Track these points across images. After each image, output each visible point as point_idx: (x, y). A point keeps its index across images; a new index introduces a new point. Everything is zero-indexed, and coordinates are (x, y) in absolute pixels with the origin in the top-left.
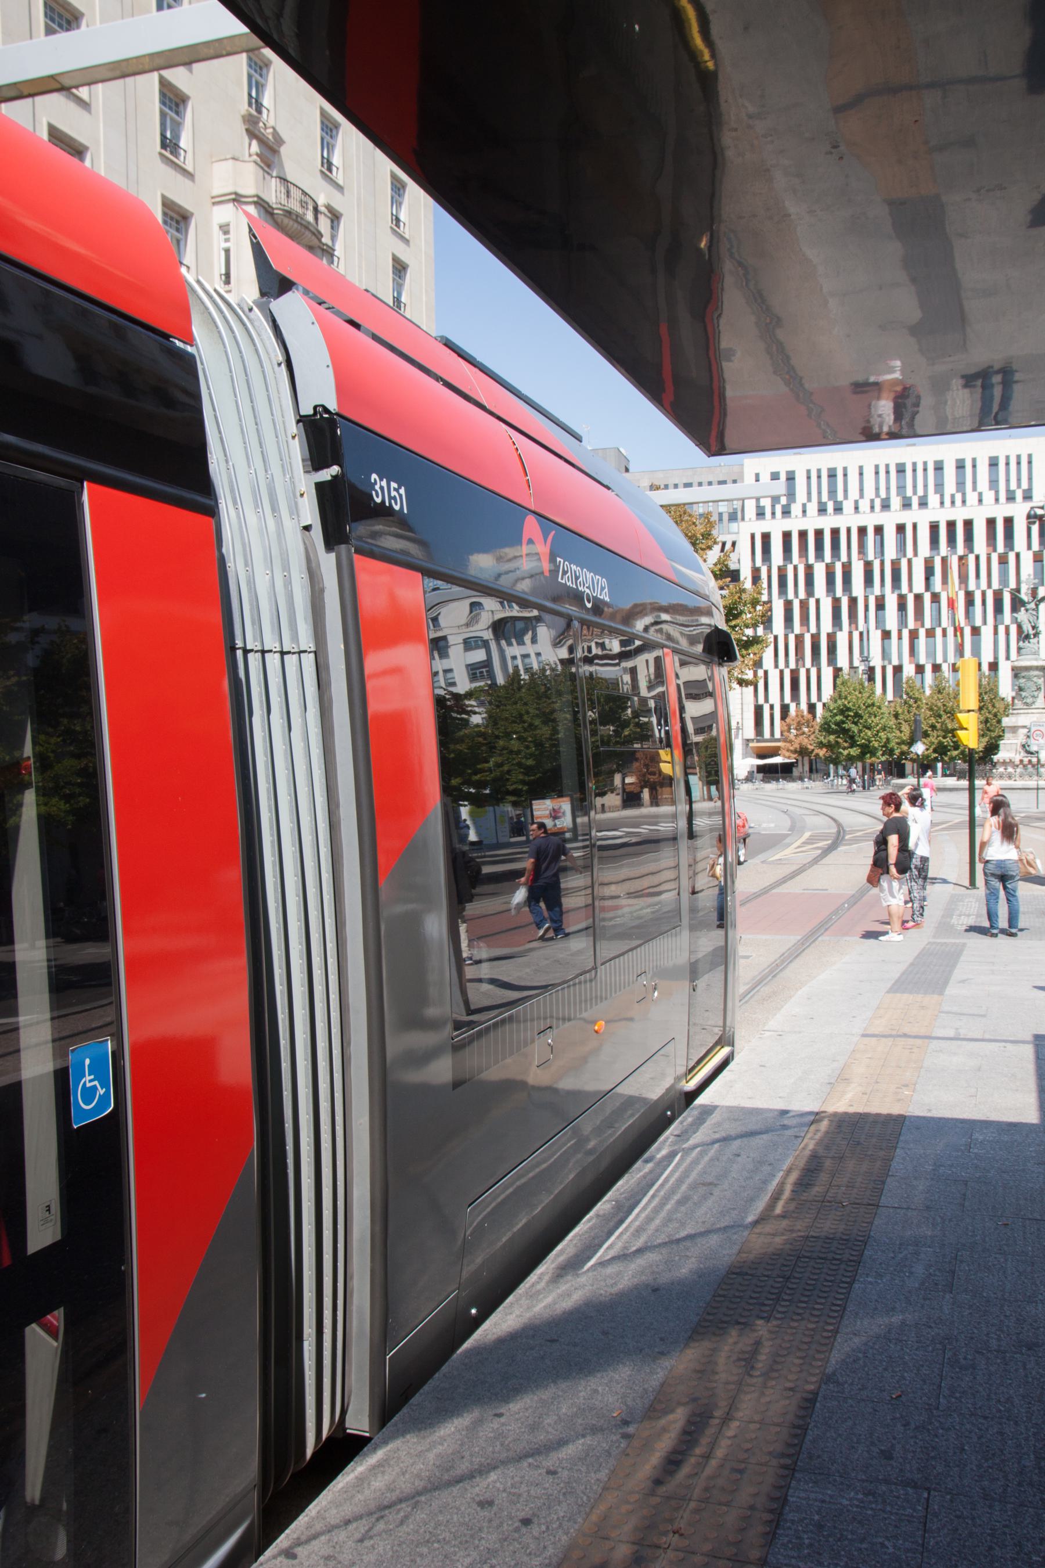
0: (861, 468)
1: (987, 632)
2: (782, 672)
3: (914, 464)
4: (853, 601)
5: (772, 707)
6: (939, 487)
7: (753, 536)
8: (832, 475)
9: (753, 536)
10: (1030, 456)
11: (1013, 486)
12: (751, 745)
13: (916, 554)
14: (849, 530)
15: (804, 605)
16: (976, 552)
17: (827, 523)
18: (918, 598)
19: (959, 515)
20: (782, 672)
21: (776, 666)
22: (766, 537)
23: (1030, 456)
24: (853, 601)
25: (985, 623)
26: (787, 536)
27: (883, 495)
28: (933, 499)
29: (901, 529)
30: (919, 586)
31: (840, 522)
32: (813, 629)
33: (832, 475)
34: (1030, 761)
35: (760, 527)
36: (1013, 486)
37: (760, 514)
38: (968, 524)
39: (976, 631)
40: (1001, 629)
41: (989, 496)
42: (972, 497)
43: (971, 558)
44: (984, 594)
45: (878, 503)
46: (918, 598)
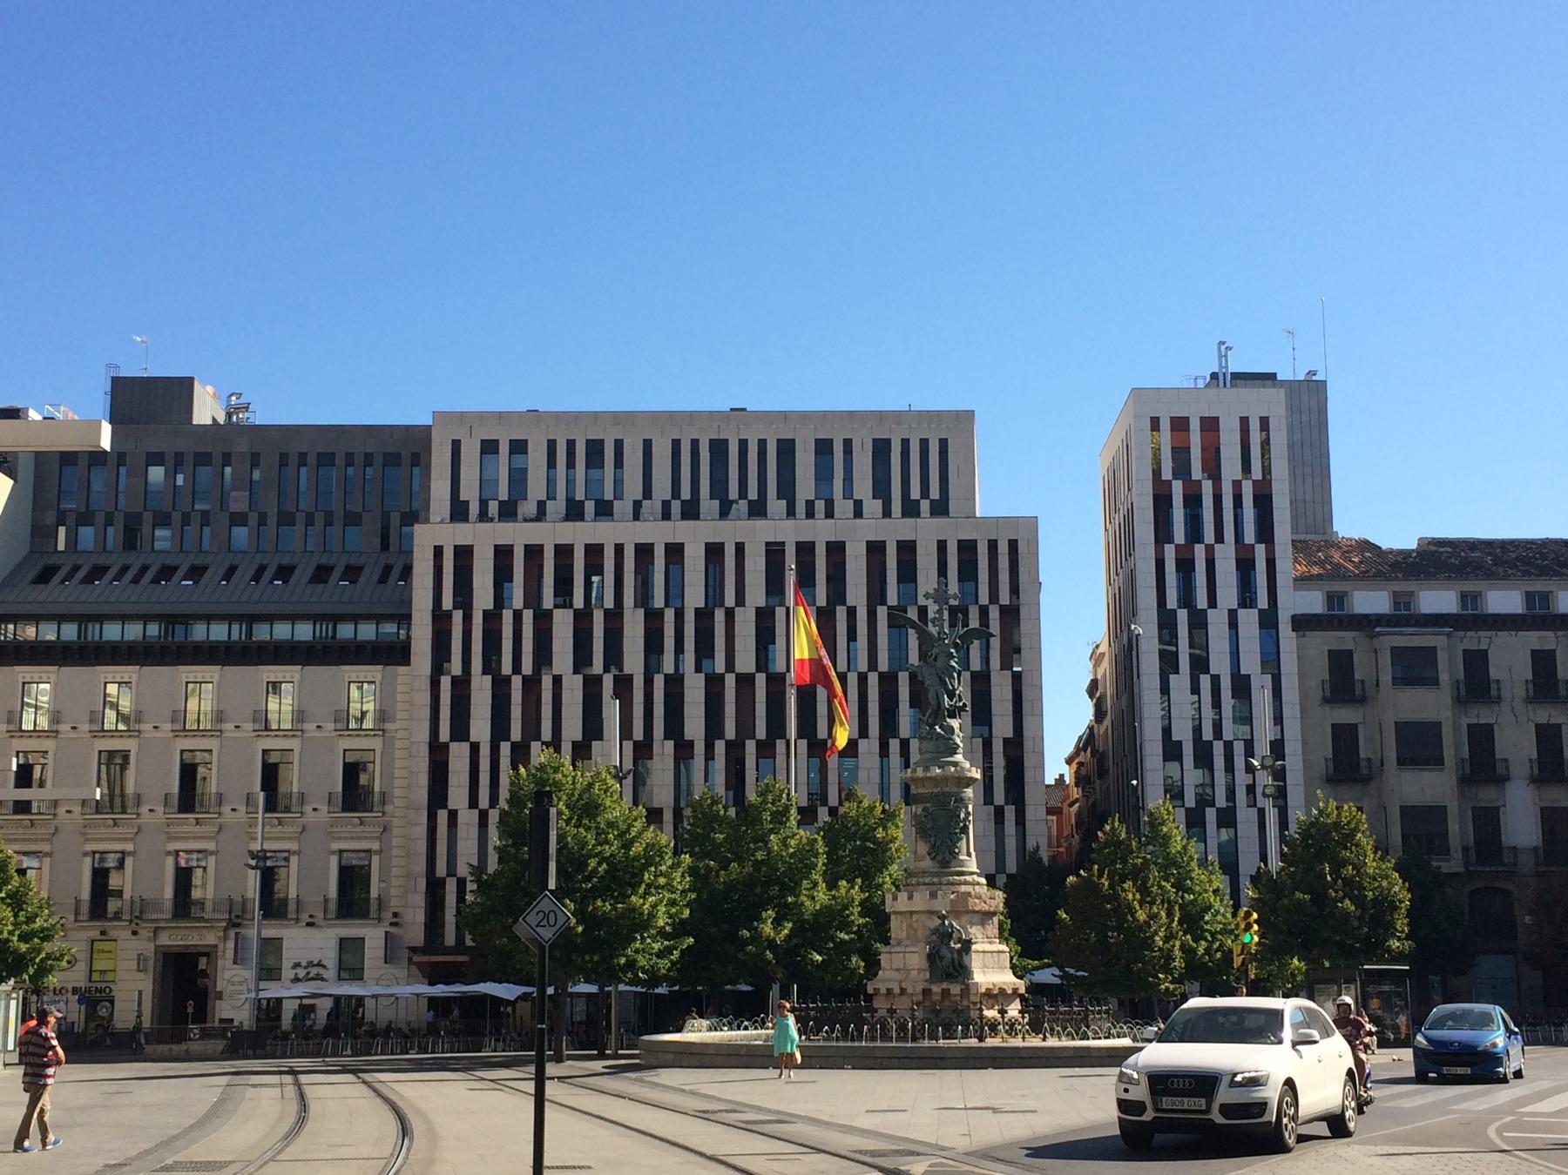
0: (648, 445)
2: (483, 816)
6: (787, 489)
7: (438, 552)
10: (943, 443)
11: (915, 494)
12: (416, 959)
13: (740, 601)
14: (619, 549)
15: (531, 684)
16: (850, 602)
18: (745, 682)
19: (821, 532)
20: (483, 816)
21: (473, 803)
22: (464, 555)
23: (943, 443)
26: (503, 554)
27: (686, 494)
28: (776, 506)
29: (714, 552)
30: (746, 661)
34: (945, 993)
35: (451, 535)
36: (915, 494)
37: (459, 512)
38: (836, 550)
40: (894, 745)
41: (873, 506)
42: (843, 507)
43: (841, 613)
45: (676, 507)
46: (745, 682)
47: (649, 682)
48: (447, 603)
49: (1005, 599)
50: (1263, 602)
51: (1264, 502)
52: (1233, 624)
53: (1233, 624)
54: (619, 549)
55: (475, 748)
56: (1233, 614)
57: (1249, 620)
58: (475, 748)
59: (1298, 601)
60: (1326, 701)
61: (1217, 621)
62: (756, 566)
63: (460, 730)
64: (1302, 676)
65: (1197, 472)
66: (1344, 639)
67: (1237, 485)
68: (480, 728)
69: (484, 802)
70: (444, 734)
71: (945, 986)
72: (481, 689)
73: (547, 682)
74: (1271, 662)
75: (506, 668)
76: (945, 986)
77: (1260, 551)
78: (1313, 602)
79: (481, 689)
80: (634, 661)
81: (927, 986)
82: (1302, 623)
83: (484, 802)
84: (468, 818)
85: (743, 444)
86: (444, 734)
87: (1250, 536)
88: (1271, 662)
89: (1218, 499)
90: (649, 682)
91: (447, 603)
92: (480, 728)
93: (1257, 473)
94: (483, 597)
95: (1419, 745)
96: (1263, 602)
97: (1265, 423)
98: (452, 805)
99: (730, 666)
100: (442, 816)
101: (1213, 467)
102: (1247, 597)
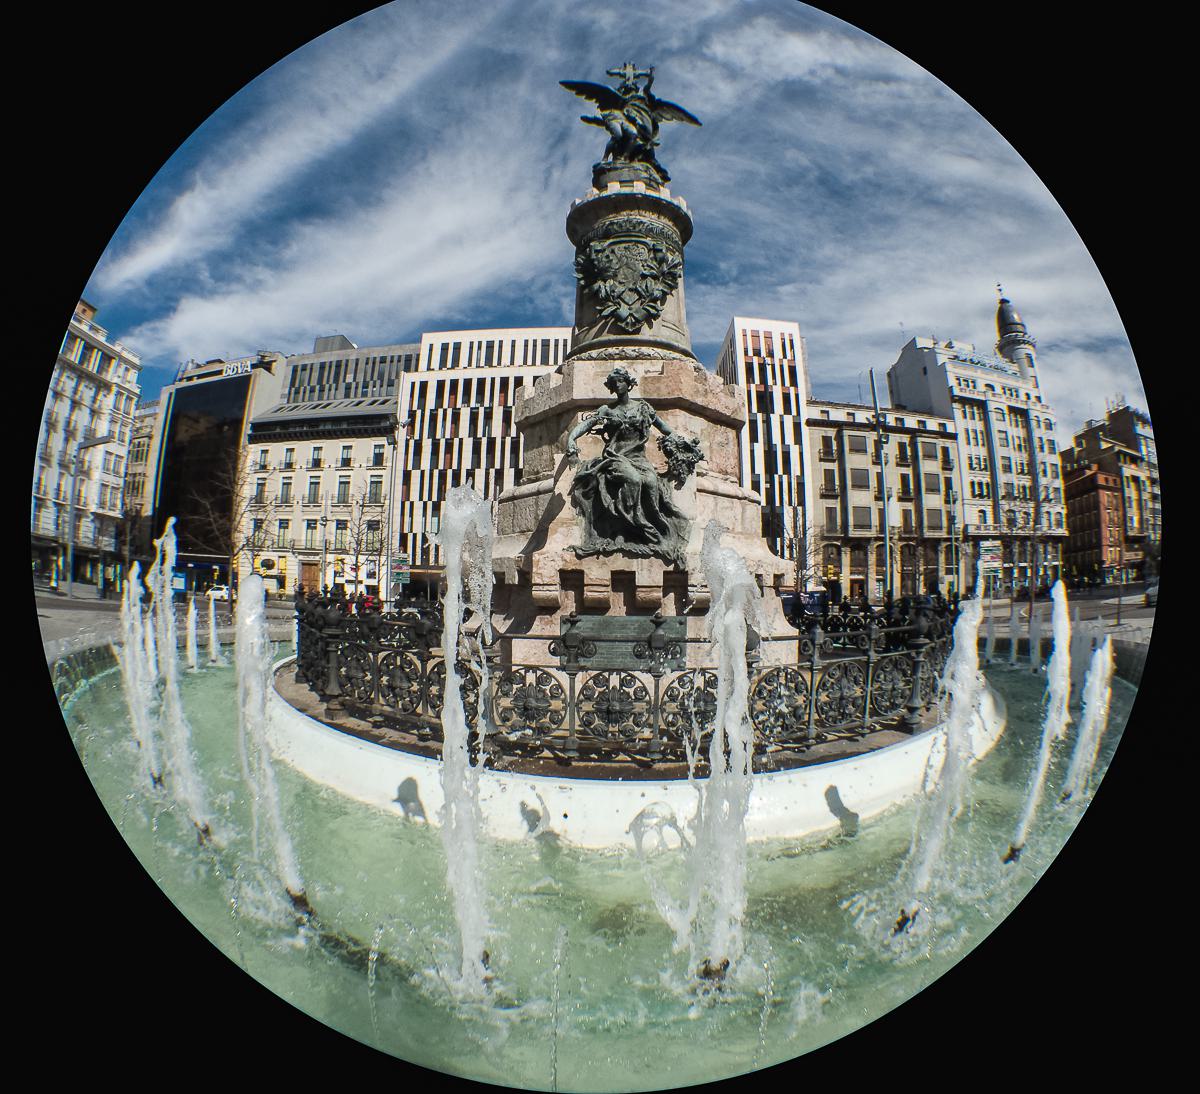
0: (514, 342)
2: (425, 504)
3: (557, 341)
4: (491, 442)
5: (415, 536)
7: (413, 384)
8: (490, 345)
9: (413, 384)
14: (493, 380)
17: (474, 374)
20: (425, 504)
21: (421, 499)
22: (424, 385)
24: (491, 442)
26: (441, 384)
31: (487, 373)
32: (455, 467)
33: (490, 345)
47: (503, 444)
48: (415, 407)
50: (794, 412)
51: (793, 371)
52: (782, 423)
53: (782, 423)
54: (493, 380)
55: (423, 472)
56: (781, 416)
57: (789, 421)
58: (423, 472)
59: (808, 412)
60: (821, 460)
61: (775, 419)
63: (417, 465)
64: (812, 446)
65: (763, 353)
66: (832, 432)
67: (781, 360)
68: (426, 464)
69: (425, 498)
70: (410, 468)
71: (620, 563)
72: (427, 444)
73: (456, 441)
74: (798, 440)
75: (438, 436)
76: (620, 563)
77: (792, 390)
78: (815, 413)
79: (427, 444)
80: (497, 430)
81: (573, 564)
82: (811, 423)
83: (425, 498)
84: (418, 506)
85: (557, 341)
87: (787, 383)
88: (798, 440)
89: (773, 366)
90: (503, 444)
91: (415, 407)
92: (426, 464)
93: (789, 356)
94: (430, 403)
95: (861, 482)
96: (794, 412)
97: (791, 335)
100: (407, 504)
101: (771, 354)
102: (787, 410)
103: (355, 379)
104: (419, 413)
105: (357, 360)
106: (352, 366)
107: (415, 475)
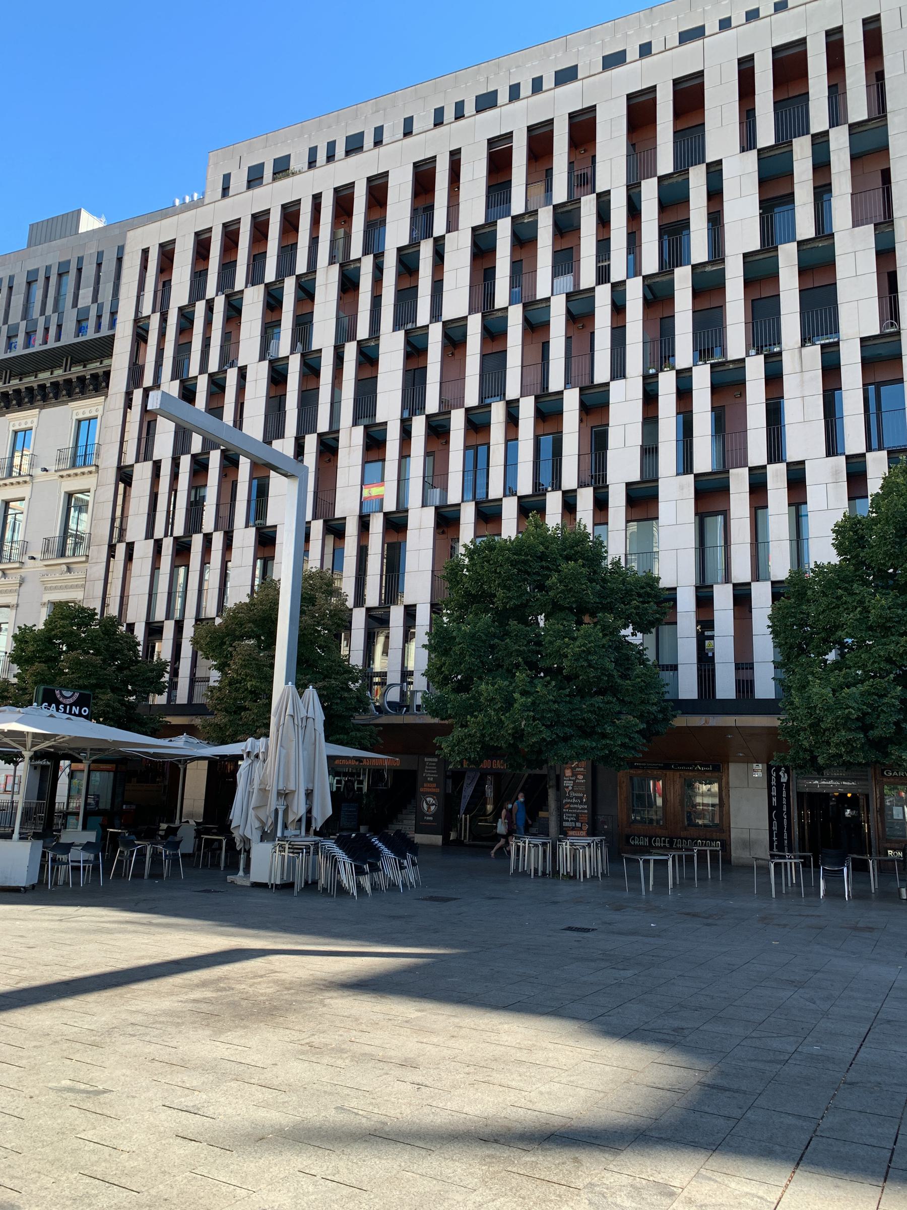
1: (625, 401)
2: (158, 544)
13: (452, 225)
20: (158, 544)
25: (618, 371)
30: (456, 302)
39: (595, 405)
44: (618, 290)
48: (146, 310)
49: (858, 108)
55: (157, 465)
62: (475, 173)
73: (232, 376)
75: (194, 369)
84: (144, 550)
86: (129, 458)
91: (146, 310)
98: (129, 538)
99: (436, 313)
100: (121, 549)
103: (95, 299)
104: (155, 320)
105: (100, 255)
106: (89, 271)
107: (142, 473)
